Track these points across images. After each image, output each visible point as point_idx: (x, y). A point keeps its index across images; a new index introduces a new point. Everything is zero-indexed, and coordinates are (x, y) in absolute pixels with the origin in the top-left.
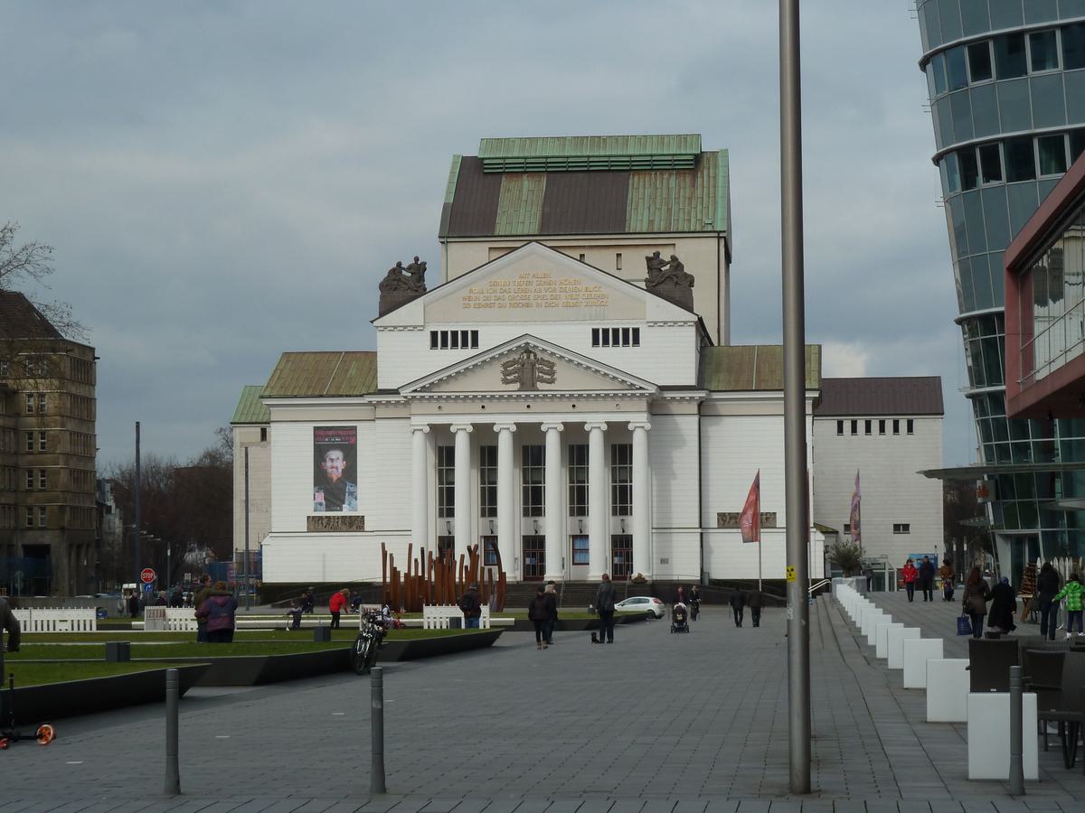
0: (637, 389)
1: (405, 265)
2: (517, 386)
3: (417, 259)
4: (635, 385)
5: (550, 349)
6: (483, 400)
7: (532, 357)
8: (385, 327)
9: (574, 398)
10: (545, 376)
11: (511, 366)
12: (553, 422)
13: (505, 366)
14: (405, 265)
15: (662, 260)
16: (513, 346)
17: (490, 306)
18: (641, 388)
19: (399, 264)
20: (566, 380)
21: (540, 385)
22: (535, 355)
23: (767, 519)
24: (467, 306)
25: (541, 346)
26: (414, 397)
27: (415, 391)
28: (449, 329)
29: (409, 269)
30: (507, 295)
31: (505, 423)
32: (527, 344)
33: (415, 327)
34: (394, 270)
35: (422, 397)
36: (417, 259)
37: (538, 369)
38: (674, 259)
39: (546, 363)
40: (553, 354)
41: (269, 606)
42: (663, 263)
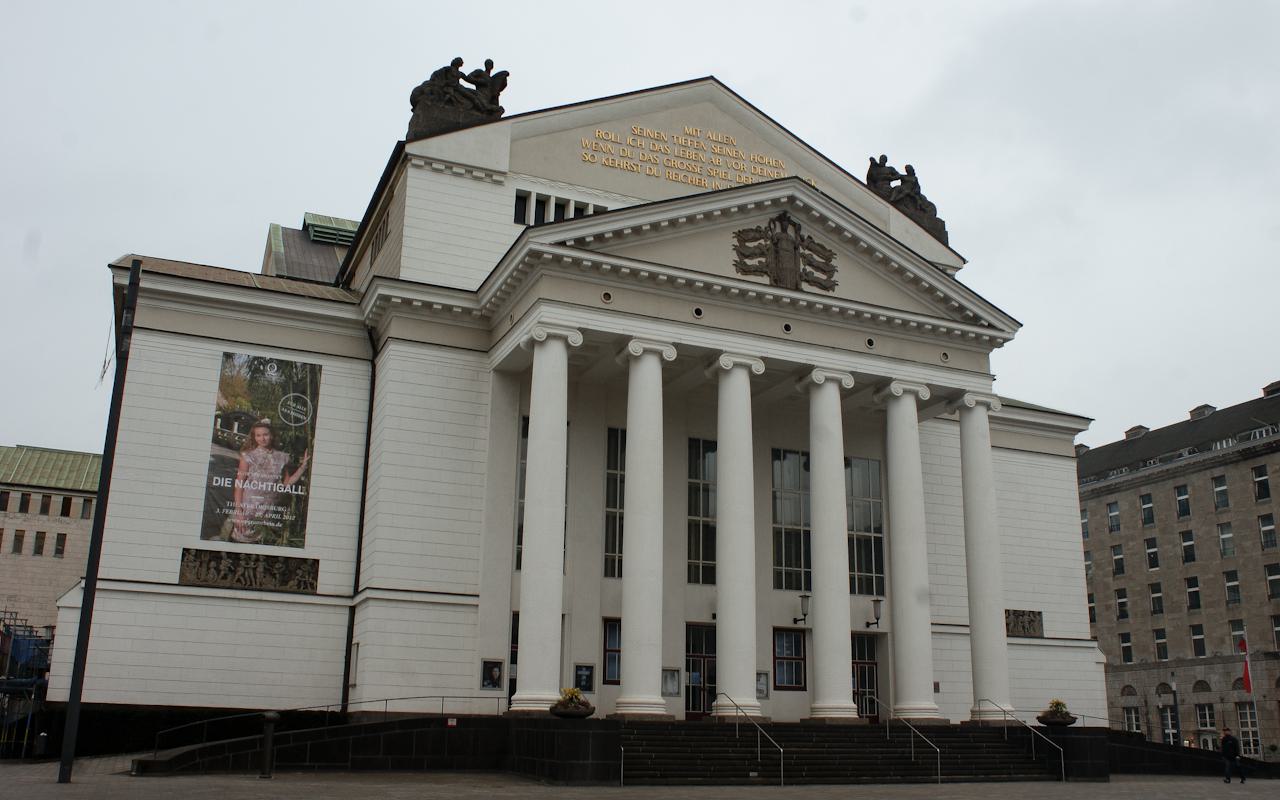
0: (982, 326)
1: (466, 69)
2: (766, 280)
3: (489, 64)
4: (980, 318)
5: (835, 219)
6: (699, 296)
7: (791, 231)
8: (429, 162)
9: (871, 326)
10: (818, 275)
11: (756, 240)
12: (835, 364)
13: (742, 236)
14: (466, 69)
15: (892, 169)
16: (766, 196)
18: (991, 326)
19: (458, 62)
20: (853, 285)
21: (805, 286)
22: (797, 228)
23: (1031, 622)
25: (819, 208)
26: (558, 259)
27: (562, 244)
28: (554, 193)
29: (476, 77)
31: (744, 349)
32: (792, 199)
34: (446, 70)
35: (577, 262)
36: (489, 64)
38: (909, 169)
39: (818, 248)
40: (838, 230)
41: (125, 762)
42: (893, 174)
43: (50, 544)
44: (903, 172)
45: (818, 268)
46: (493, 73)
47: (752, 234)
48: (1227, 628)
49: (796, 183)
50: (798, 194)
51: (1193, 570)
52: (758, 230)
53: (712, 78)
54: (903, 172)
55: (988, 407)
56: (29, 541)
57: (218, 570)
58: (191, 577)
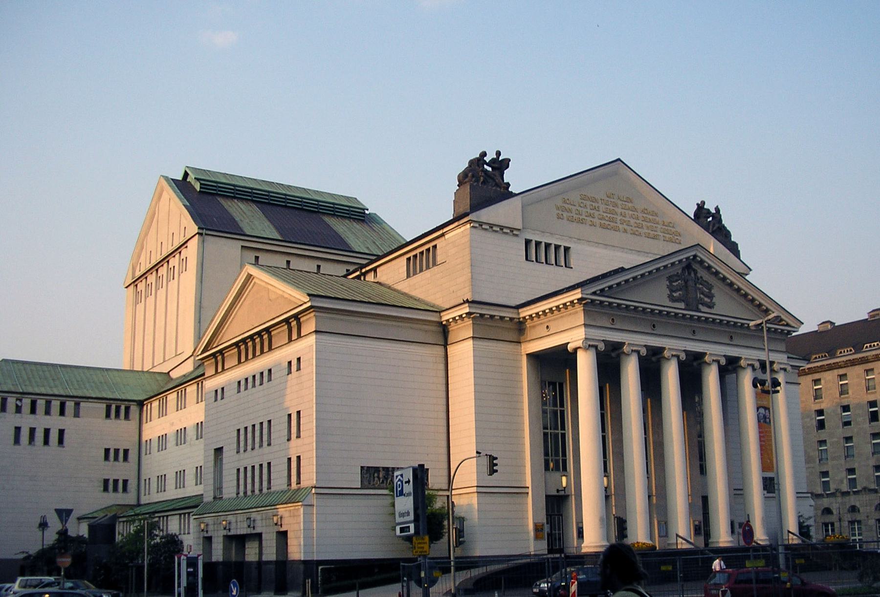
1: (487, 159)
2: (682, 305)
3: (498, 154)
4: (782, 320)
9: (732, 330)
10: (706, 299)
11: (677, 281)
13: (670, 279)
14: (487, 159)
17: (581, 222)
18: (788, 325)
19: (484, 154)
21: (700, 306)
22: (696, 272)
24: (559, 217)
26: (593, 301)
27: (594, 293)
30: (596, 213)
33: (512, 229)
35: (602, 302)
36: (498, 154)
37: (699, 289)
40: (717, 273)
43: (54, 437)
44: (713, 211)
45: (706, 296)
46: (500, 159)
47: (676, 278)
48: (844, 473)
49: (699, 248)
50: (699, 254)
51: (823, 435)
52: (677, 275)
53: (619, 160)
54: (713, 211)
55: (785, 370)
56: (39, 435)
57: (379, 478)
58: (366, 483)
